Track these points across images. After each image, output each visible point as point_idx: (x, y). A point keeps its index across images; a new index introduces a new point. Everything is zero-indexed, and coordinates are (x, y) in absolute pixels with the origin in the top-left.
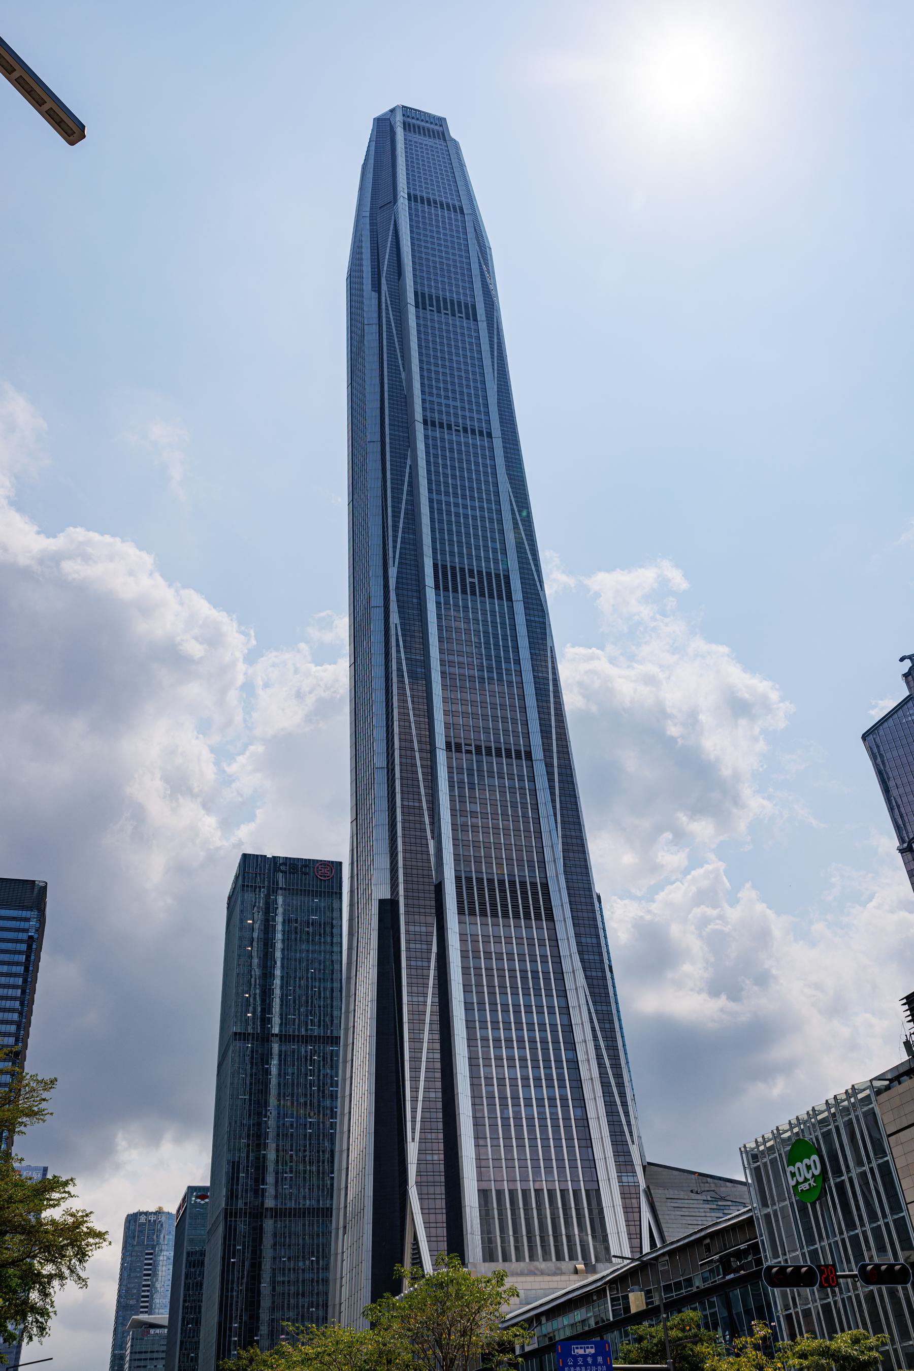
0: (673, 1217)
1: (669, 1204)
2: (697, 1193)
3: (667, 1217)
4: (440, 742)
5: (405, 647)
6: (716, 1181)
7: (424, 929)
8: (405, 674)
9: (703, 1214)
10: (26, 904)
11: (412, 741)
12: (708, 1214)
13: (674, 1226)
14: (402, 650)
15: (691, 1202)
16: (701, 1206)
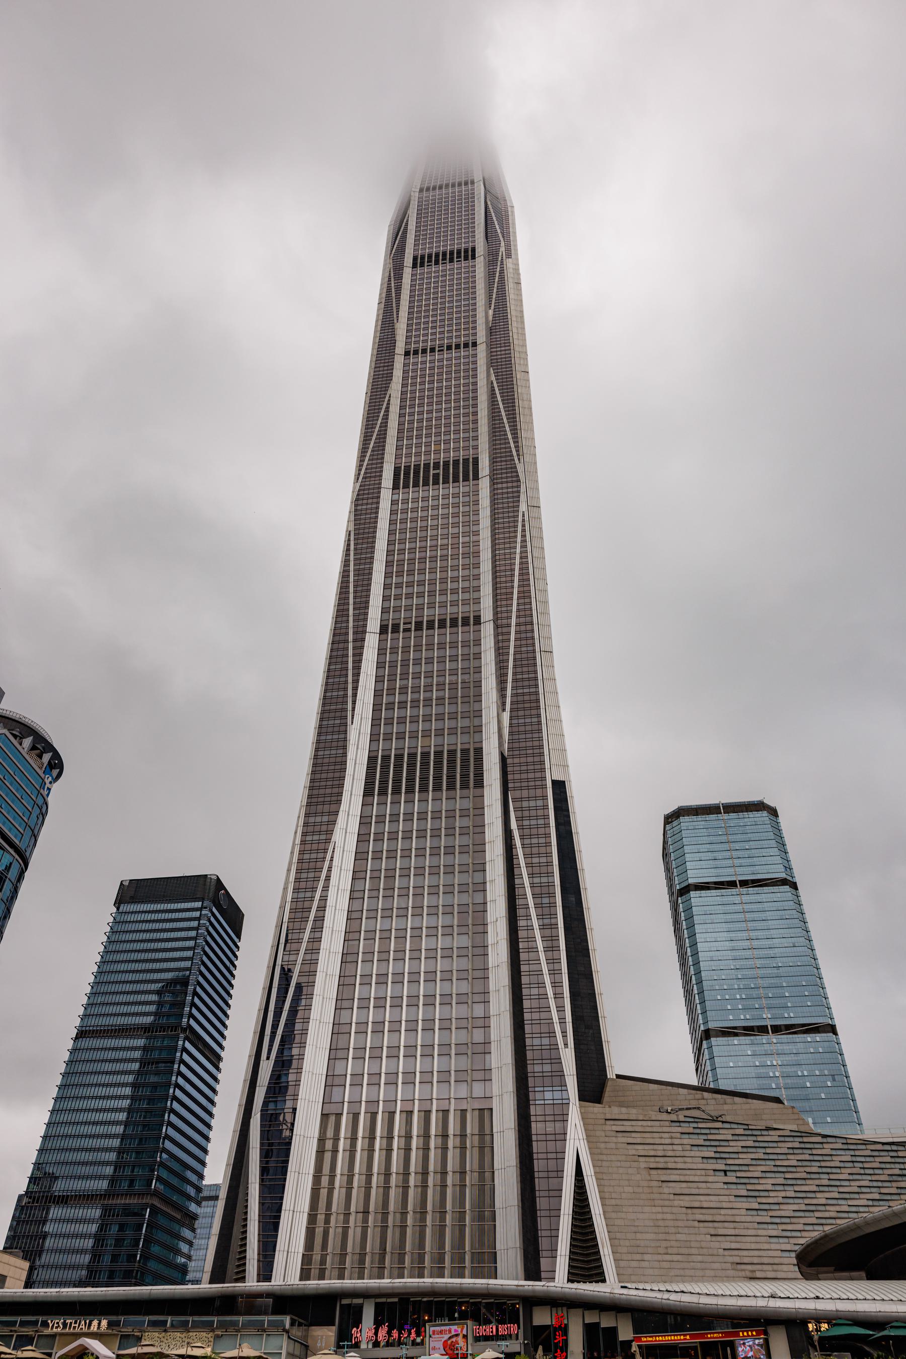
0: (613, 1146)
1: (607, 1128)
2: (667, 1112)
3: (603, 1145)
4: (373, 623)
5: (355, 549)
6: (719, 1096)
7: (325, 819)
8: (352, 574)
9: (668, 1141)
10: (198, 896)
11: (347, 634)
12: (676, 1141)
13: (613, 1158)
15: (649, 1123)
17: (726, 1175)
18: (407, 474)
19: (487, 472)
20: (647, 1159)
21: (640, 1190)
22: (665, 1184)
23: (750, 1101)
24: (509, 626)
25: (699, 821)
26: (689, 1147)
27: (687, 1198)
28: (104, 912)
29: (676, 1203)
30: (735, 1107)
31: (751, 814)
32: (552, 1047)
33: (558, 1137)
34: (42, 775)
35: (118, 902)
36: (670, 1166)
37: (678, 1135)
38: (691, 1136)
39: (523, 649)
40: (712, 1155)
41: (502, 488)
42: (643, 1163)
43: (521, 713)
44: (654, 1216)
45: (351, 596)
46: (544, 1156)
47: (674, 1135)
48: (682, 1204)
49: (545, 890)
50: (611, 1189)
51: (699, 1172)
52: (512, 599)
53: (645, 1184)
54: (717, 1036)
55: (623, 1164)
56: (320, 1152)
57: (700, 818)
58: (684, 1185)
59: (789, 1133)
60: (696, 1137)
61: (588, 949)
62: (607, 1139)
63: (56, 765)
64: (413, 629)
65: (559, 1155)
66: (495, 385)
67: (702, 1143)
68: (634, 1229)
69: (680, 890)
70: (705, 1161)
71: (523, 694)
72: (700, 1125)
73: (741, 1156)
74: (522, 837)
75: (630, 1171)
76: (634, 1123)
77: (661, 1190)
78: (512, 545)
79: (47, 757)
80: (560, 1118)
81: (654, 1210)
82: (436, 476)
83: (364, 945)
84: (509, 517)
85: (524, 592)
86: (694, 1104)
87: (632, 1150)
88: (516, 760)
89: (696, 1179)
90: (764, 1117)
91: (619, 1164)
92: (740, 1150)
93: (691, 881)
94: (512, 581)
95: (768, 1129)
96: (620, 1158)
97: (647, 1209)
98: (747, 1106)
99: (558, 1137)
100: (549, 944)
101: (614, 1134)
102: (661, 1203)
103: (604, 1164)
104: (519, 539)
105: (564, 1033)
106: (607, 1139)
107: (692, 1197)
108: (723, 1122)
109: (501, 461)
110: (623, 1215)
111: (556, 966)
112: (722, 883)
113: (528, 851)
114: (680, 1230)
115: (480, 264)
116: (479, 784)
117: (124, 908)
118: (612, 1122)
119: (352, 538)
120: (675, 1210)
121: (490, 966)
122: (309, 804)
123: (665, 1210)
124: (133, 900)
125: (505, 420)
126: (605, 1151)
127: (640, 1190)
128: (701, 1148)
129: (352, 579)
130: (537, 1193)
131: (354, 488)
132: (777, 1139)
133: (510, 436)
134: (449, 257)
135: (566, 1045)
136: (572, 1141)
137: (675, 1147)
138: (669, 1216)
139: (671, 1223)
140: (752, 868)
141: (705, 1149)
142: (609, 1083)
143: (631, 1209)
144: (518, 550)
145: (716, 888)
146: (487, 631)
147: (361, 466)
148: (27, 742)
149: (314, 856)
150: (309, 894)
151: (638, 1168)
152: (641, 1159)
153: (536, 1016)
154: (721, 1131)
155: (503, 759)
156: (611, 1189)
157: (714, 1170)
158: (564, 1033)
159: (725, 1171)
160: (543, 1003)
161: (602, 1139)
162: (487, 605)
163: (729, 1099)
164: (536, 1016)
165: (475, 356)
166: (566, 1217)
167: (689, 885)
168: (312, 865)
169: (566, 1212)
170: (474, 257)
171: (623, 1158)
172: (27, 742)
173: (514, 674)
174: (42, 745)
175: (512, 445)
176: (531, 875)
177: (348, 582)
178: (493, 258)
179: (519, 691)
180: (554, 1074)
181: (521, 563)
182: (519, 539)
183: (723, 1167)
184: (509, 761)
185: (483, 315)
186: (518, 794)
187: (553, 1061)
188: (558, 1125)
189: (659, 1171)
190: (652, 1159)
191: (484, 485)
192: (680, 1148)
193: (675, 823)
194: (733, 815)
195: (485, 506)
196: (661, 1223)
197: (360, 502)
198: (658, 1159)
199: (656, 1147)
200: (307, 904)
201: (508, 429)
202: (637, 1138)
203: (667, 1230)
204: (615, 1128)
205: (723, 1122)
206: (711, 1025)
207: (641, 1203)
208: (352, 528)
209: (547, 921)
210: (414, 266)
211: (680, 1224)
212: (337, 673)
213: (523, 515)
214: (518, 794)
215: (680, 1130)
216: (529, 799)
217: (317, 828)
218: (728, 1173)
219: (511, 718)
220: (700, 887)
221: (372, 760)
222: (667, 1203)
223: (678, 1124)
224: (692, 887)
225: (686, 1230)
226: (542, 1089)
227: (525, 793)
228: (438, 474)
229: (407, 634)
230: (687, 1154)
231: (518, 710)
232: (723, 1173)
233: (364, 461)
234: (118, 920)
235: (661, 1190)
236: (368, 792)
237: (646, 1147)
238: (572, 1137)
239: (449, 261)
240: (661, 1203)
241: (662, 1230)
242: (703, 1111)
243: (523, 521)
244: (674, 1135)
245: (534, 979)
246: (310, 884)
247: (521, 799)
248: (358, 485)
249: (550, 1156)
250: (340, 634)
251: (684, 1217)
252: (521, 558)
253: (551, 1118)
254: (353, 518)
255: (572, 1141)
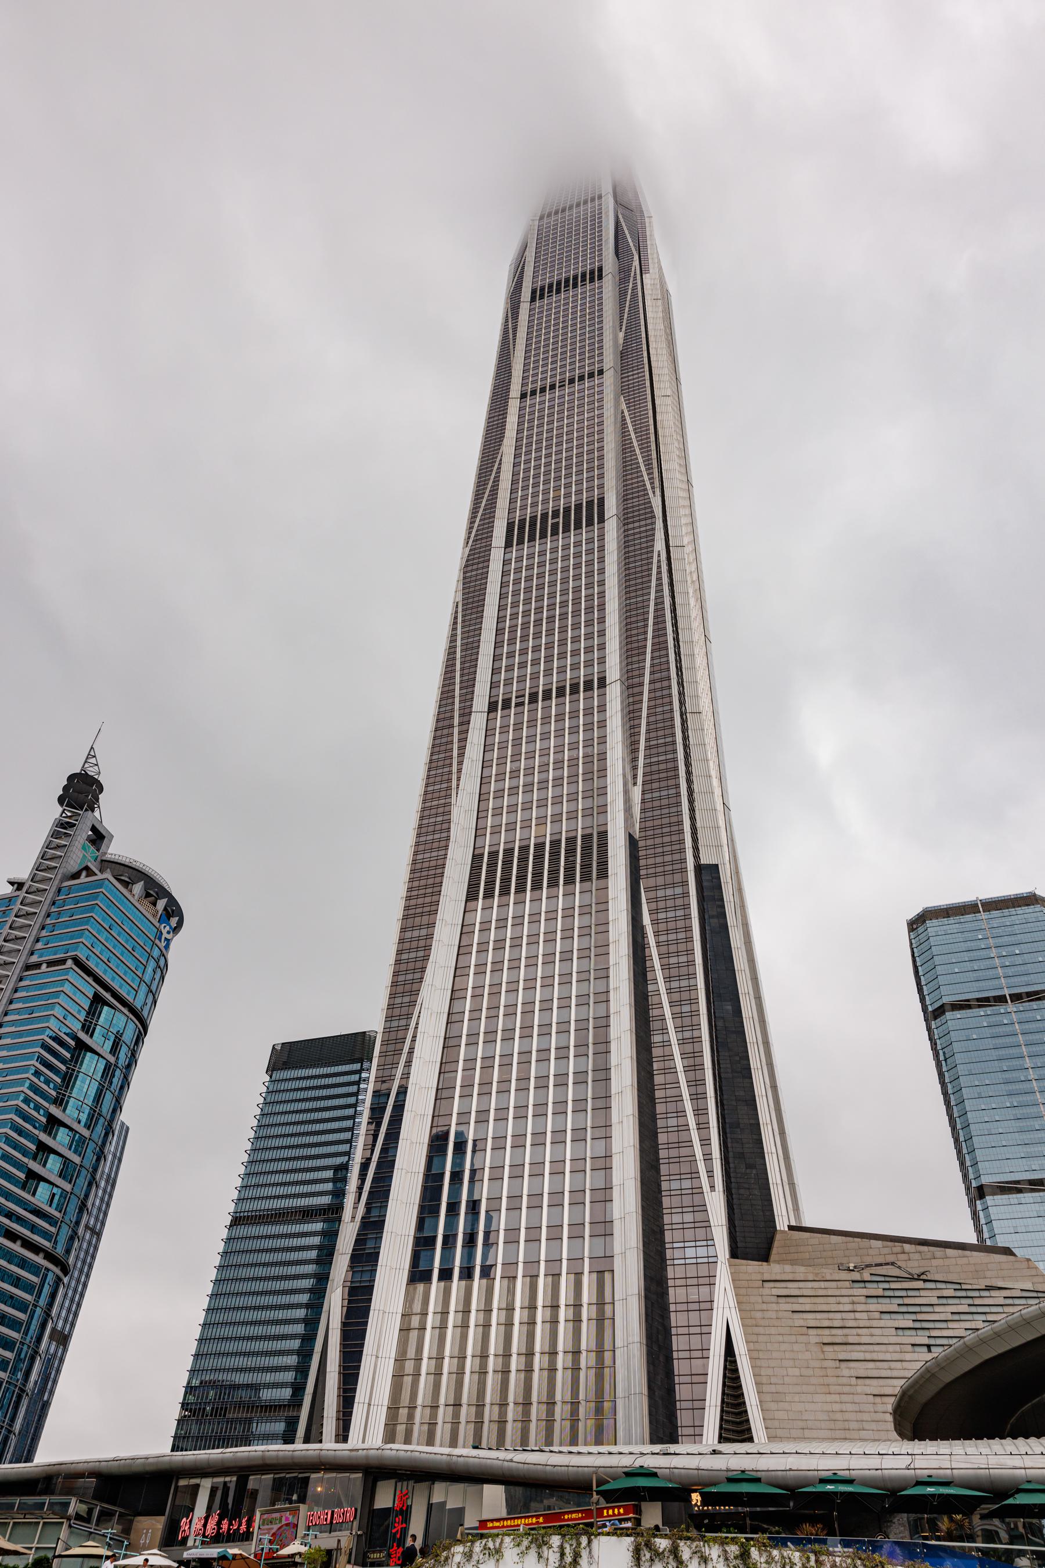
0: (773, 1315)
1: (766, 1291)
3: (759, 1315)
5: (463, 621)
8: (458, 650)
10: (356, 1056)
11: (452, 717)
13: (773, 1331)
14: (459, 626)
15: (822, 1285)
16: (844, 1292)
17: (930, 1351)
18: (522, 528)
19: (614, 511)
20: (820, 1331)
21: (810, 1372)
22: (844, 1365)
23: (968, 1253)
24: (642, 684)
25: (951, 925)
26: (877, 1315)
27: (874, 1382)
28: (255, 1082)
29: (859, 1389)
30: (947, 1262)
31: (1020, 911)
32: (695, 1191)
33: (703, 1306)
34: (157, 925)
35: (271, 1069)
36: (851, 1340)
37: (863, 1299)
38: (881, 1300)
39: (658, 710)
40: (911, 1324)
41: (634, 528)
42: (814, 1337)
43: (655, 785)
44: (828, 1407)
45: (458, 674)
46: (685, 1330)
47: (855, 1299)
48: (868, 1390)
49: (685, 996)
50: (770, 1372)
51: (891, 1348)
52: (645, 653)
53: (817, 1364)
54: (994, 1194)
55: (786, 1338)
56: (405, 1330)
57: (952, 920)
58: (871, 1365)
59: (1019, 1294)
60: (887, 1300)
61: (750, 1069)
62: (764, 1307)
63: (173, 912)
64: (527, 702)
65: (705, 1330)
66: (626, 413)
67: (895, 1308)
68: (801, 1424)
69: (934, 1011)
70: (900, 1332)
71: (658, 763)
72: (893, 1286)
73: (951, 1325)
74: (657, 934)
75: (796, 1347)
76: (801, 1285)
77: (838, 1372)
78: (645, 591)
79: (161, 904)
80: (706, 1281)
81: (829, 1398)
82: (555, 526)
83: (463, 1077)
84: (641, 560)
85: (659, 643)
86: (891, 1258)
87: (799, 1320)
88: (650, 842)
89: (888, 1357)
90: (988, 1274)
91: (780, 1338)
92: (950, 1317)
93: (946, 1000)
94: (646, 633)
95: (989, 1288)
96: (781, 1330)
97: (818, 1398)
98: (965, 1261)
99: (703, 1306)
100: (691, 1062)
101: (774, 1299)
102: (839, 1389)
103: (761, 1338)
104: (654, 583)
105: (710, 1173)
106: (764, 1307)
107: (881, 1382)
108: (925, 1281)
109: (633, 498)
110: (786, 1406)
111: (700, 1089)
112: (987, 999)
113: (664, 949)
114: (866, 1426)
115: (609, 286)
116: (603, 874)
117: (277, 1075)
118: (772, 1284)
119: (460, 609)
120: (857, 1398)
121: (613, 1092)
122: (405, 917)
123: (845, 1398)
124: (286, 1065)
125: (638, 451)
126: (762, 1322)
127: (810, 1372)
128: (894, 1316)
129: (458, 655)
130: (676, 1378)
131: (463, 553)
132: (1002, 1301)
133: (643, 468)
134: (573, 282)
135: (712, 1187)
136: (720, 1311)
137: (858, 1315)
138: (850, 1407)
139: (852, 1416)
140: (1025, 978)
141: (900, 1316)
142: (778, 1237)
143: (797, 1398)
144: (653, 596)
145: (980, 1006)
146: (614, 693)
147: (471, 528)
148: (138, 888)
149: (410, 977)
150: (403, 1022)
151: (807, 1343)
152: (811, 1332)
153: (674, 1153)
154: (922, 1293)
155: (632, 843)
156: (770, 1372)
157: (913, 1345)
158: (710, 1173)
159: (929, 1346)
160: (683, 1136)
161: (758, 1307)
162: (613, 664)
163: (938, 1251)
164: (674, 1153)
165: (601, 385)
166: (713, 1409)
167: (943, 1006)
168: (408, 987)
169: (713, 1403)
170: (600, 277)
171: (787, 1330)
172: (138, 888)
173: (647, 740)
174: (155, 890)
175: (646, 478)
176: (668, 979)
177: (454, 659)
178: (623, 273)
179: (653, 760)
180: (697, 1225)
181: (656, 611)
182: (654, 583)
183: (926, 1341)
184: (641, 844)
185: (612, 338)
186: (651, 882)
187: (696, 1209)
188: (705, 1290)
189: (836, 1347)
190: (827, 1332)
191: (612, 528)
192: (864, 1316)
193: (921, 930)
194: (995, 913)
195: (611, 549)
196: (839, 1416)
197: (470, 568)
198: (834, 1331)
199: (831, 1315)
200: (400, 1035)
201: (640, 460)
202: (806, 1304)
203: (846, 1425)
204: (775, 1292)
205: (925, 1281)
206: (985, 1180)
207: (812, 1389)
208: (459, 598)
209: (687, 1035)
210: (533, 299)
211: (866, 1417)
212: (440, 763)
213: (659, 555)
214: (651, 882)
215: (865, 1292)
216: (665, 886)
217: (414, 944)
218: (933, 1349)
219: (643, 793)
220: (957, 1006)
221: (477, 858)
222: (846, 1389)
223: (862, 1285)
224: (947, 1007)
225: (873, 1426)
226: (682, 1245)
227: (660, 880)
228: (558, 523)
229: (519, 709)
230: (875, 1323)
231: (651, 782)
232: (925, 1349)
233: (474, 522)
234: (271, 1089)
235: (838, 1372)
236: (471, 895)
237: (818, 1316)
238: (721, 1305)
239: (583, 296)
240: (839, 1389)
241: (839, 1425)
242: (899, 1267)
243: (659, 561)
244: (855, 1299)
245: (671, 1107)
246: (404, 1010)
247: (656, 888)
248: (468, 549)
249: (692, 1330)
250: (444, 719)
251: (871, 1408)
252: (656, 604)
253: (694, 1281)
254: (461, 587)
255: (720, 1311)
